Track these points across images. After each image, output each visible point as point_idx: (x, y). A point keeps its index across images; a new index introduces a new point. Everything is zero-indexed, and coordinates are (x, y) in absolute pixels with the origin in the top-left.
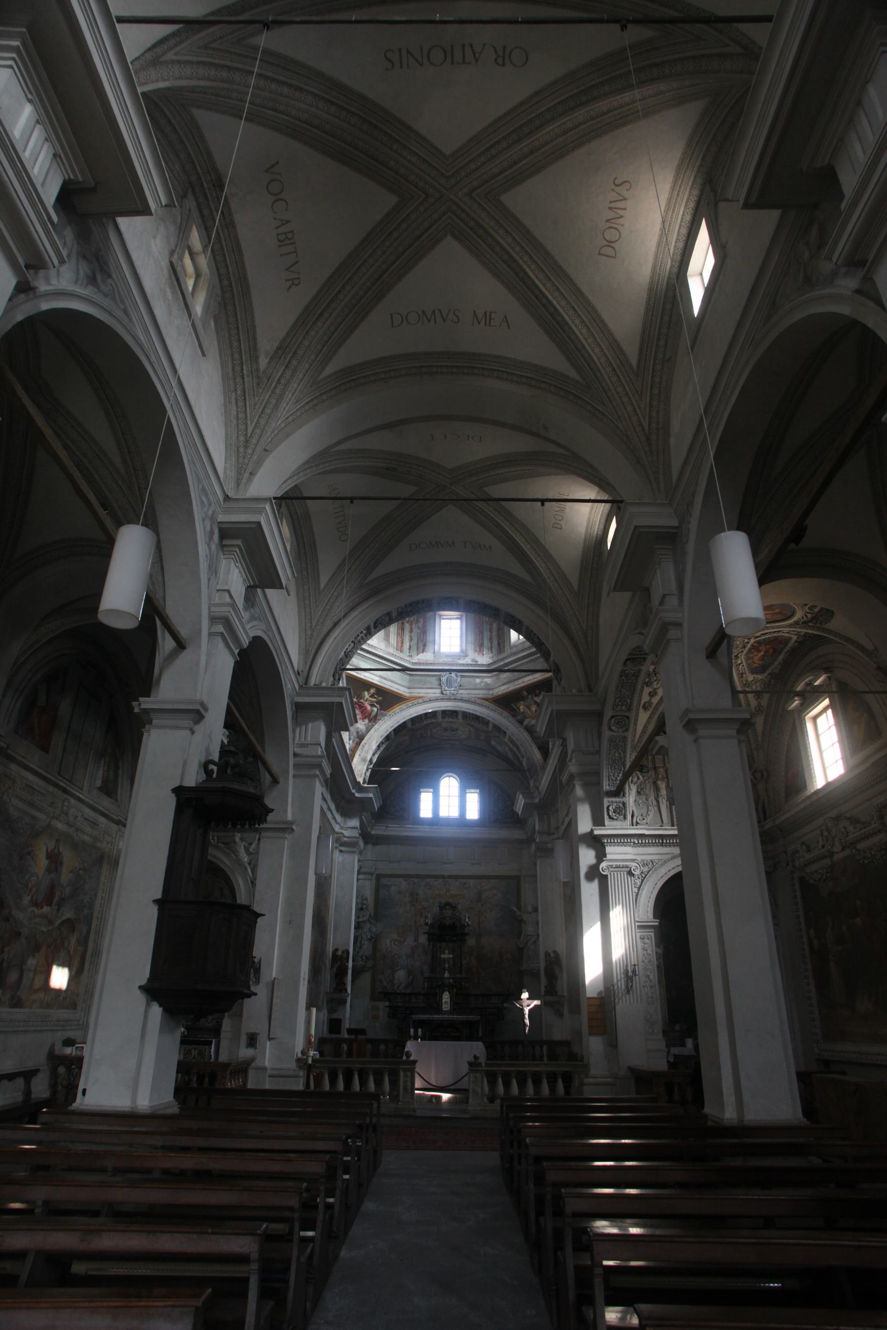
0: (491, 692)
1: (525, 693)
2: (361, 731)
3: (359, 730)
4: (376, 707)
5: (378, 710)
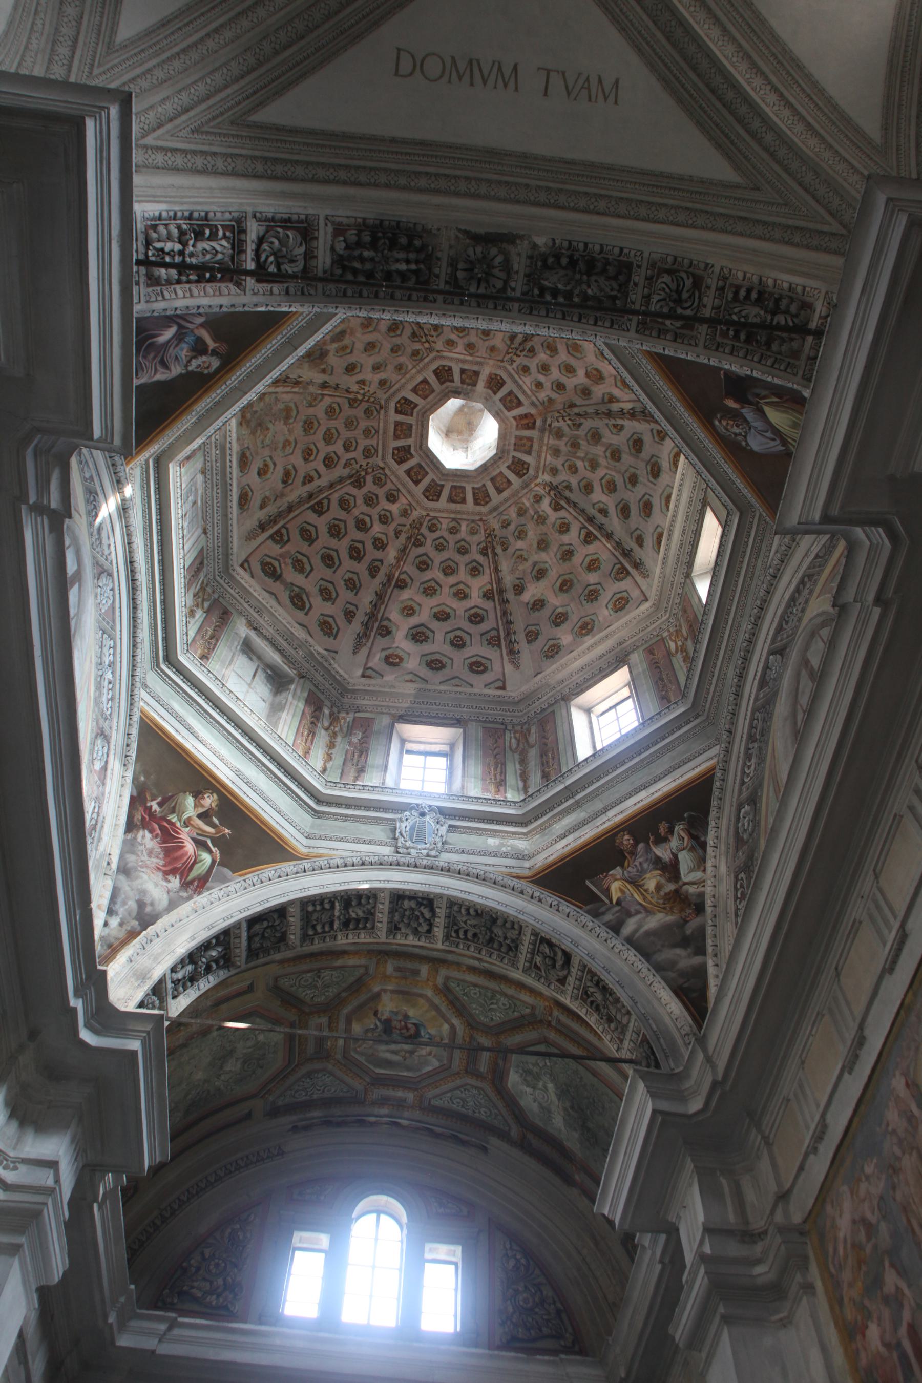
0: (527, 864)
1: (626, 840)
2: (152, 904)
3: (148, 900)
4: (210, 852)
5: (214, 862)
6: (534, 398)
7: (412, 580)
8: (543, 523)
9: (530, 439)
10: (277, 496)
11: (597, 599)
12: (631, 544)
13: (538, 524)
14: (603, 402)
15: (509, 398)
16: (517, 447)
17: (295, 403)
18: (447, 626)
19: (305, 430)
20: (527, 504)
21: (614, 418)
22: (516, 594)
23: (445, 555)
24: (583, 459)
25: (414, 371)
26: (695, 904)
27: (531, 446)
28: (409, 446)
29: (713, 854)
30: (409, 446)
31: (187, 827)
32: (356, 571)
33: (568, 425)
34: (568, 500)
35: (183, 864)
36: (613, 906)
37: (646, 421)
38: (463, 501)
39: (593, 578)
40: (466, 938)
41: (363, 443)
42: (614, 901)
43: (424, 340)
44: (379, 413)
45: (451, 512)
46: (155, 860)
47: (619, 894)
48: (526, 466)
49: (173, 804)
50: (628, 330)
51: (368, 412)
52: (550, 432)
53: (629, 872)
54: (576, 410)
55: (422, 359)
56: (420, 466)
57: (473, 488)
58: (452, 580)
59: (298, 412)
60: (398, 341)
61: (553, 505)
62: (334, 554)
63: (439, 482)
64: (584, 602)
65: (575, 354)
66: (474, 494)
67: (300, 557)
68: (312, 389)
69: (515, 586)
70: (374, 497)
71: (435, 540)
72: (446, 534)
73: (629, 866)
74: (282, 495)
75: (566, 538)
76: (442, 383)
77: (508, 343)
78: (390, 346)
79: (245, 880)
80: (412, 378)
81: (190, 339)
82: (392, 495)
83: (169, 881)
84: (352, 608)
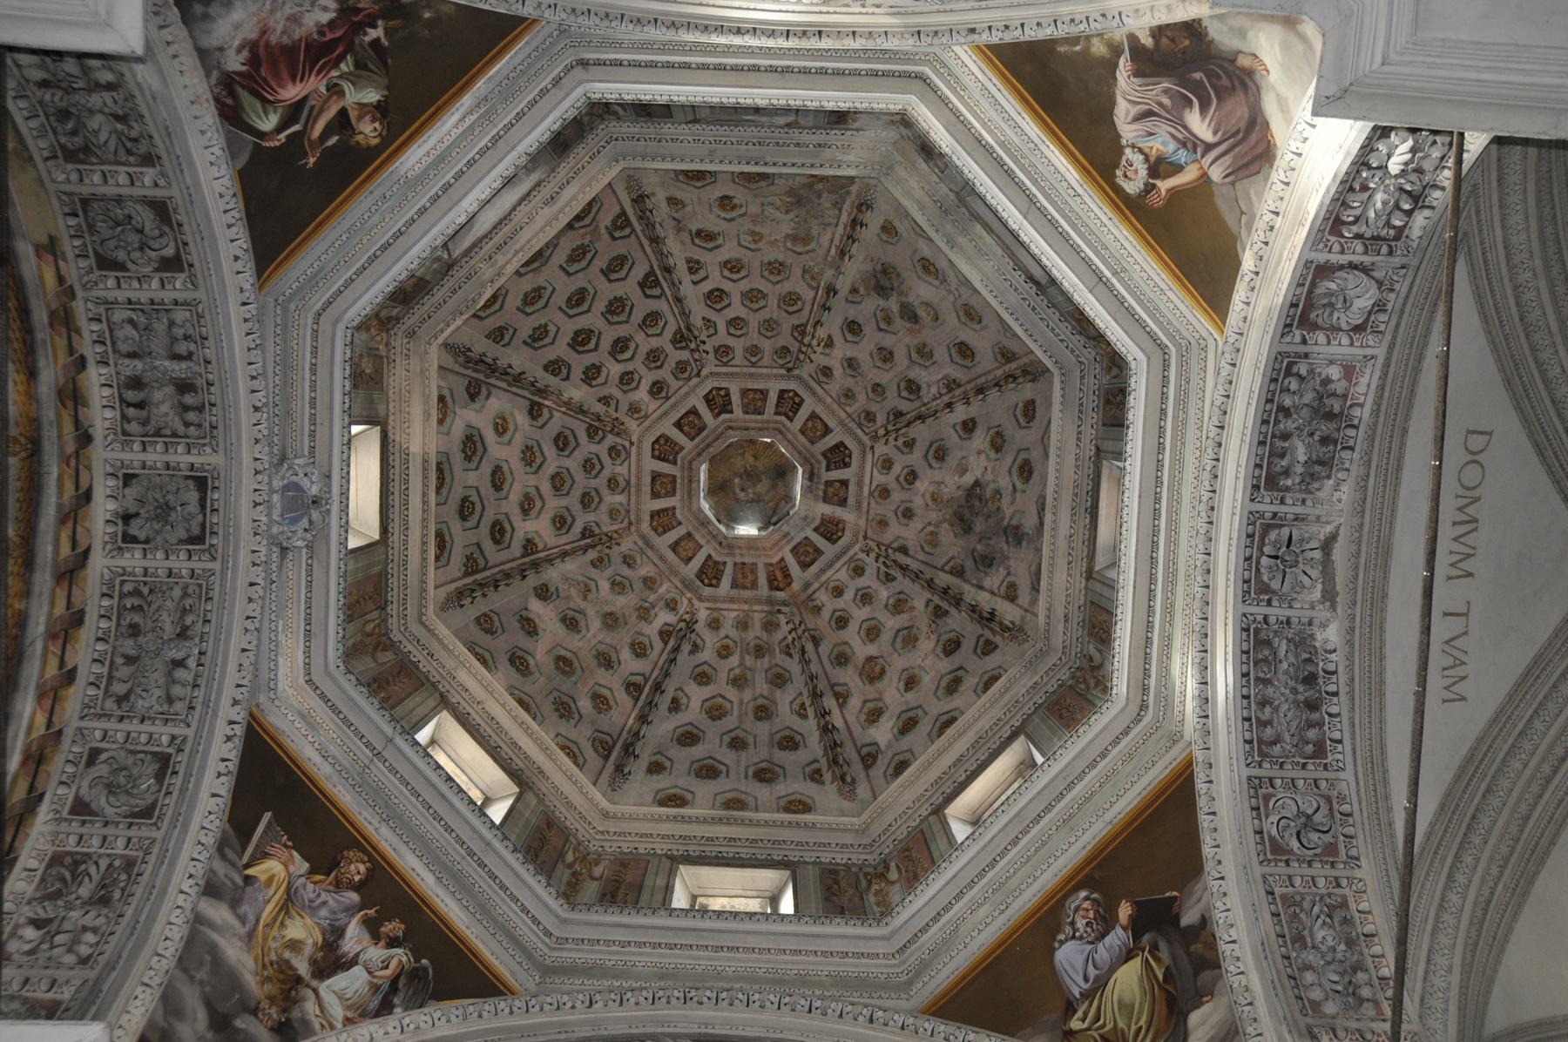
1: (357, 869)
4: (279, 129)
5: (262, 135)
6: (816, 585)
7: (542, 427)
8: (640, 618)
9: (754, 585)
10: (679, 222)
11: (561, 716)
12: (645, 753)
13: (638, 609)
14: (832, 686)
15: (811, 550)
16: (740, 567)
17: (814, 250)
18: (486, 488)
19: (770, 263)
20: (662, 590)
21: (812, 704)
22: (535, 589)
23: (579, 475)
24: (742, 664)
25: (843, 415)
26: (288, 1019)
27: (745, 588)
28: (731, 412)
29: (390, 1029)
30: (731, 412)
31: (328, 89)
32: (557, 343)
33: (785, 638)
34: (676, 649)
35: (265, 80)
36: (240, 873)
37: (825, 750)
38: (655, 495)
39: (585, 704)
40: (122, 609)
41: (738, 346)
42: (250, 872)
43: (890, 427)
44: (782, 366)
45: (639, 478)
46: (280, 28)
47: (263, 878)
48: (714, 582)
49: (371, 66)
50: (1248, 765)
51: (784, 351)
52: (769, 613)
53: (305, 886)
54: (809, 646)
55: (860, 425)
56: (701, 429)
57: (674, 508)
58: (546, 487)
59: (800, 254)
60: (892, 392)
61: (666, 628)
62: (585, 307)
63: (679, 456)
64: (551, 698)
65: (899, 639)
66: (666, 510)
67: (589, 256)
68: (829, 274)
69: (546, 586)
70: (659, 363)
71: (597, 456)
72: (606, 473)
73: (315, 883)
74: (679, 226)
75: (626, 654)
76: (824, 454)
77: (895, 545)
78: (883, 382)
79: (234, 195)
80: (833, 413)
81: (1182, 156)
82: (660, 390)
83: (239, 51)
84: (507, 338)
